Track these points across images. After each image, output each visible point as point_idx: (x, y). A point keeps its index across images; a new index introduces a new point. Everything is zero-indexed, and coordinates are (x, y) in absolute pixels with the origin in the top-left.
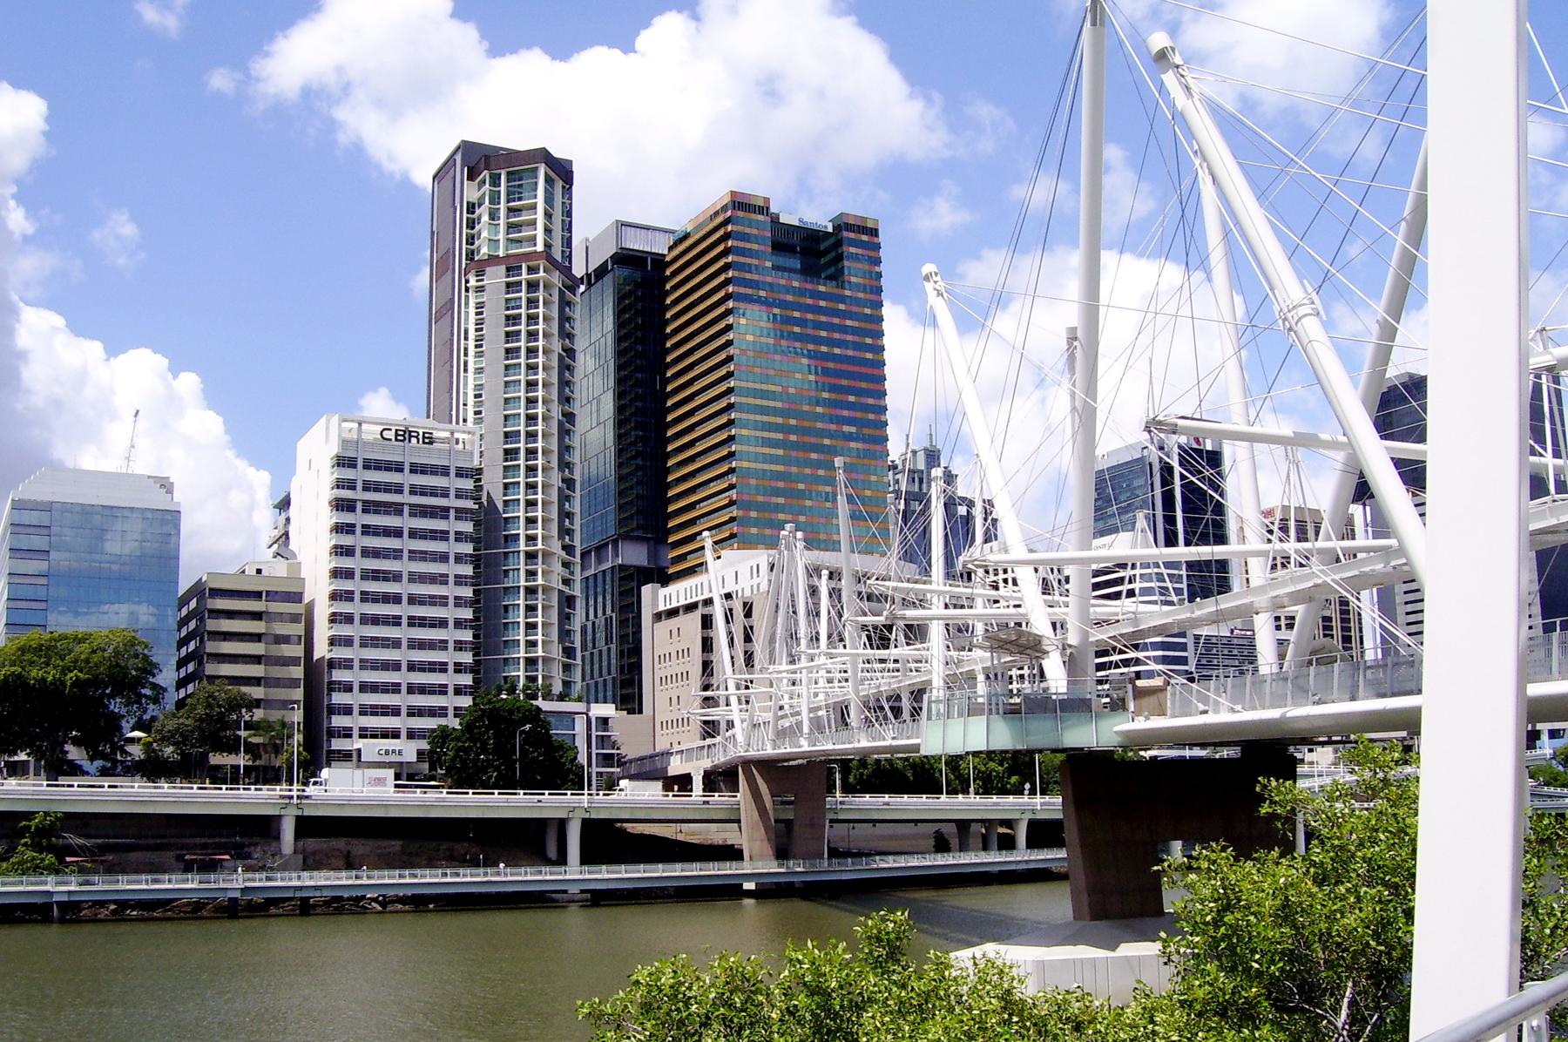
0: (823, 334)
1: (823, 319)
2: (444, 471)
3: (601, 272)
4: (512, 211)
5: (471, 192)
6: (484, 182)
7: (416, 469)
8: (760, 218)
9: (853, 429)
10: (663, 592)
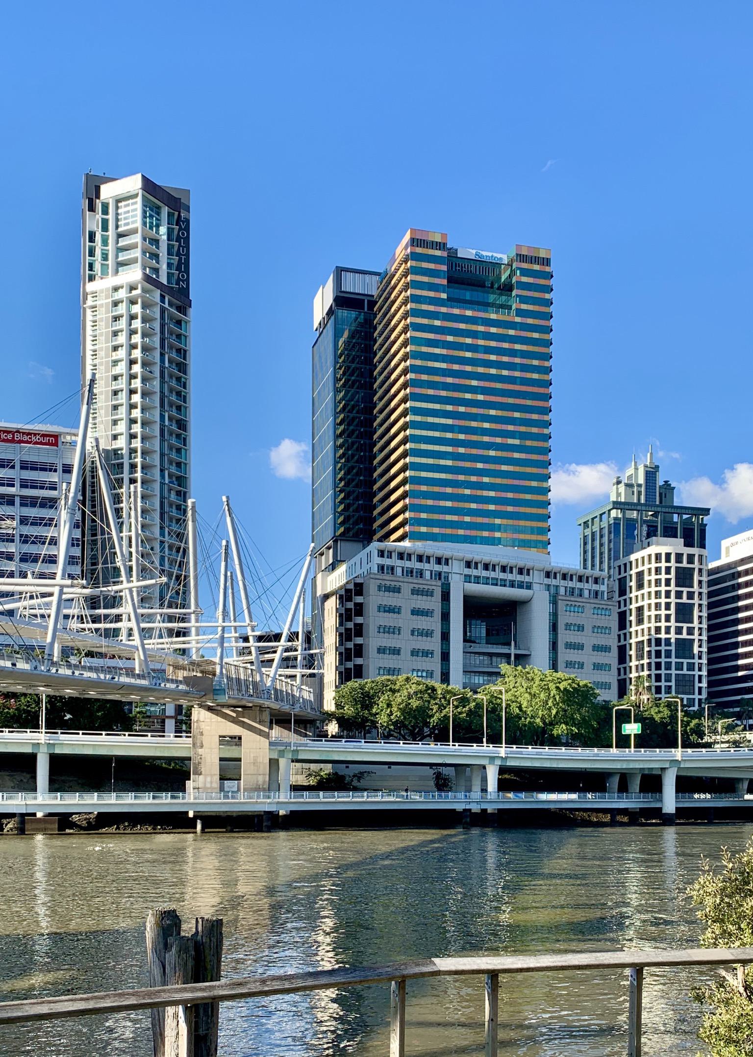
0: (493, 357)
1: (493, 344)
9: (517, 442)
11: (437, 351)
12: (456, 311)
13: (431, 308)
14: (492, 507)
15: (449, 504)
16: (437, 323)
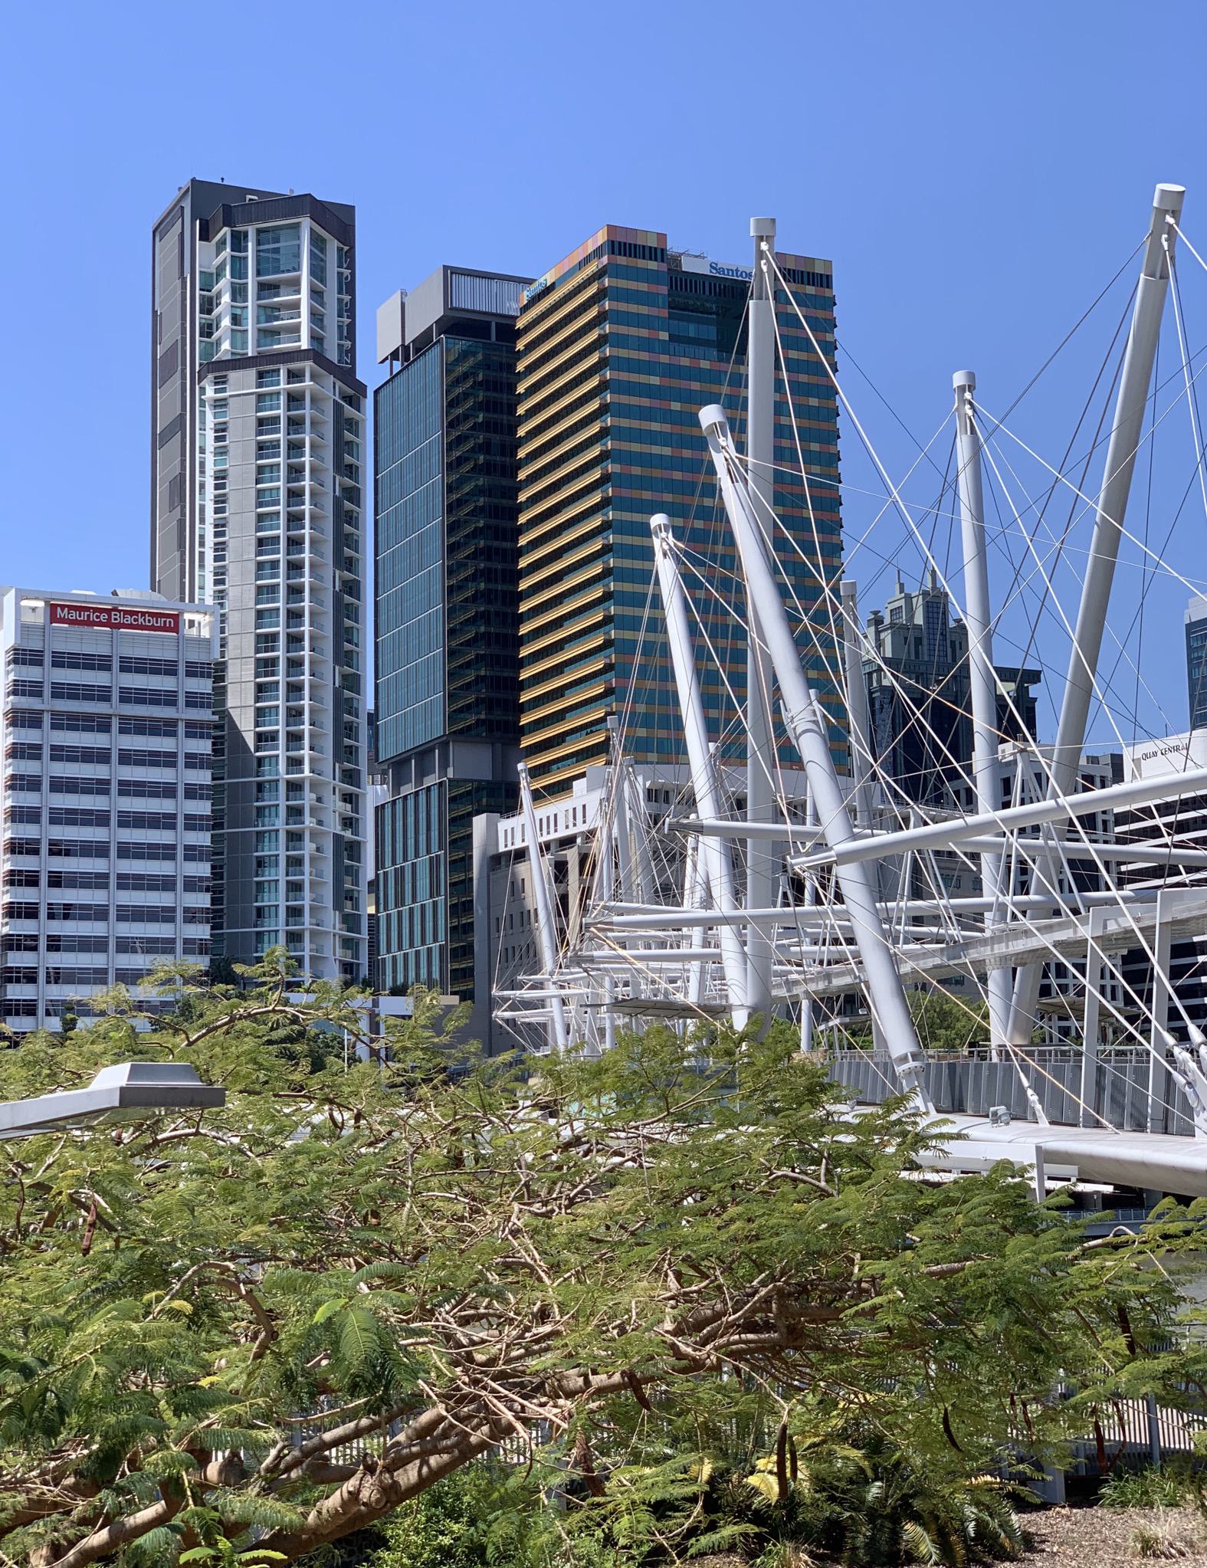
2: (168, 669)
3: (423, 343)
4: (265, 289)
5: (210, 256)
6: (223, 242)
7: (129, 665)
8: (653, 265)
10: (504, 825)
11: (655, 426)
13: (644, 356)
16: (655, 380)
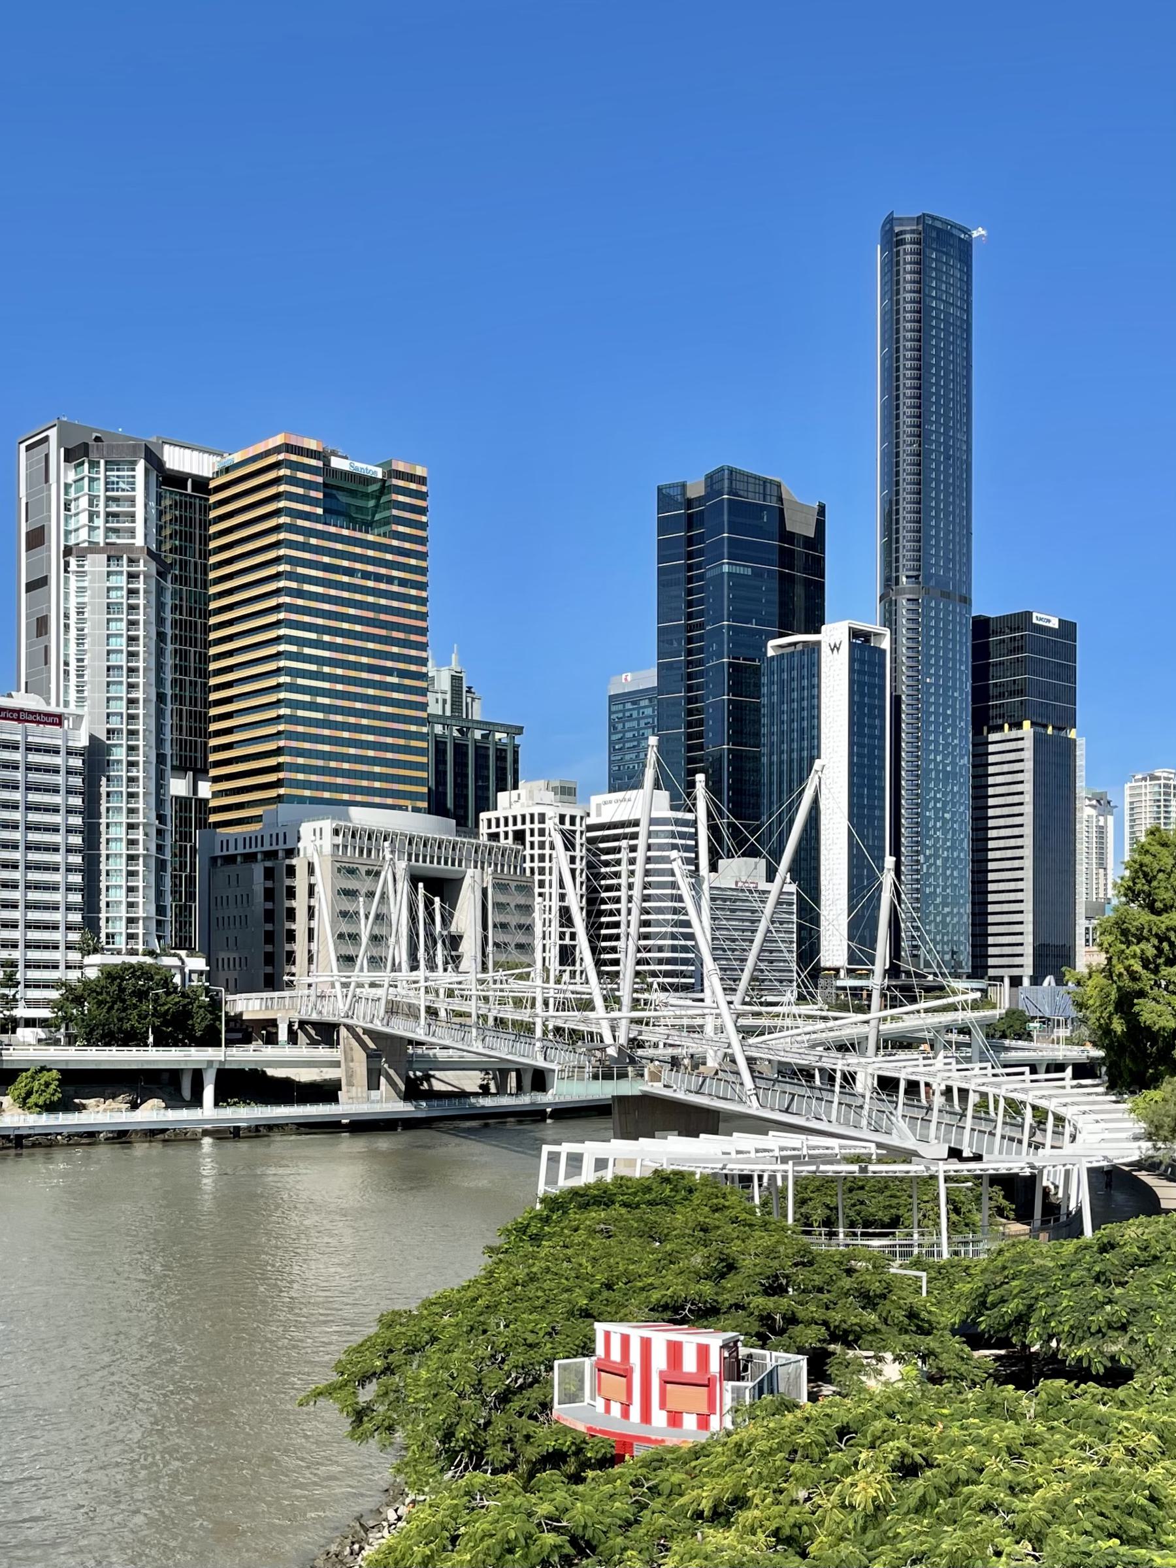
12: (333, 529)
14: (371, 753)
15: (327, 748)
